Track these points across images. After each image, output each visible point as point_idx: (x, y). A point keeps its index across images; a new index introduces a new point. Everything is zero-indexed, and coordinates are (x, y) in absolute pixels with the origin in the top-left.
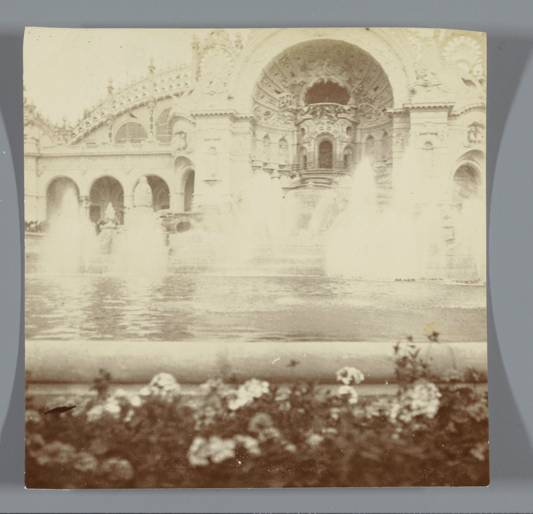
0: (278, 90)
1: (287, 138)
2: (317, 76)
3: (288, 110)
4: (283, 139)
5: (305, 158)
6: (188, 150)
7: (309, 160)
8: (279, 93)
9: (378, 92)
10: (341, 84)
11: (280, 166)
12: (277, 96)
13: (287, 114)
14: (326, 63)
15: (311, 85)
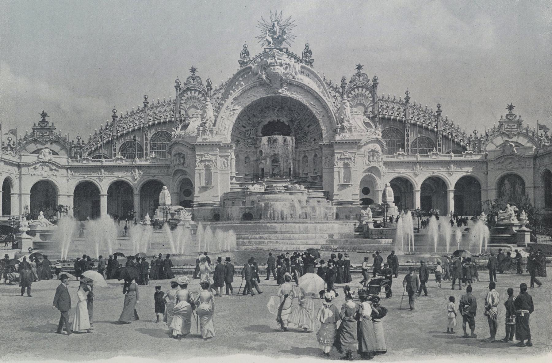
0: (244, 125)
1: (250, 156)
2: (271, 117)
3: (250, 138)
4: (247, 157)
5: (263, 169)
6: (186, 165)
7: (265, 171)
8: (245, 127)
9: (311, 128)
10: (286, 123)
11: (246, 175)
12: (244, 130)
13: (250, 141)
14: (276, 109)
15: (266, 123)
